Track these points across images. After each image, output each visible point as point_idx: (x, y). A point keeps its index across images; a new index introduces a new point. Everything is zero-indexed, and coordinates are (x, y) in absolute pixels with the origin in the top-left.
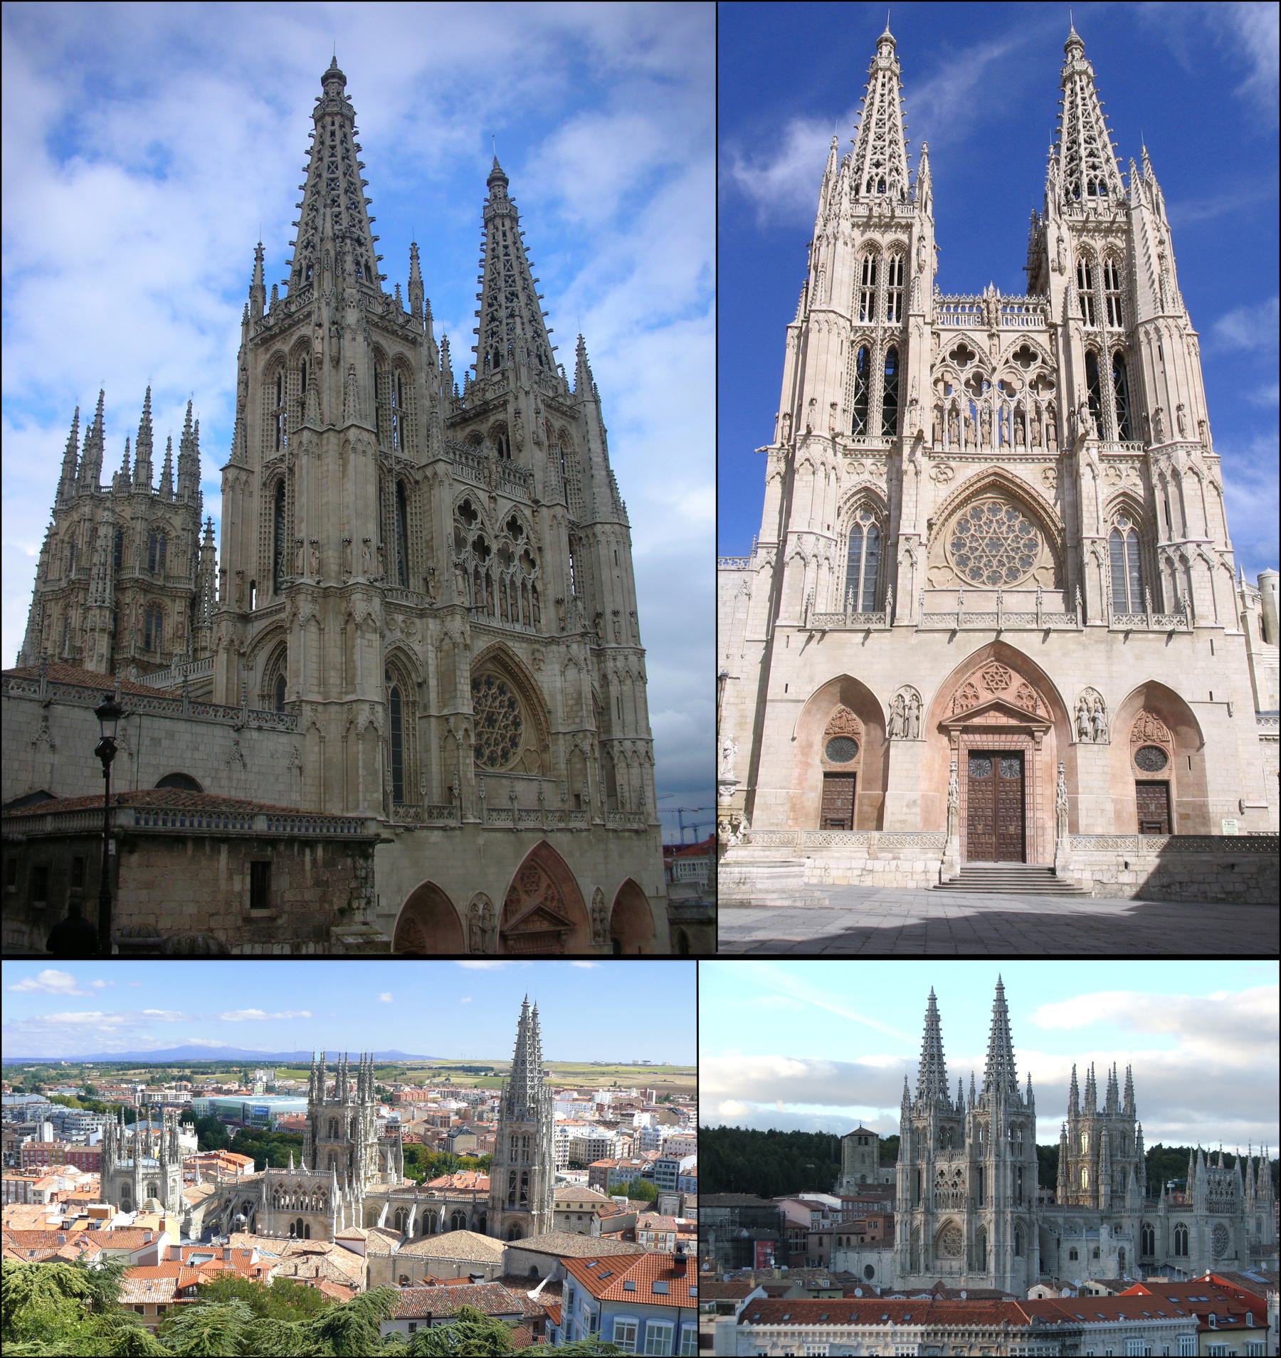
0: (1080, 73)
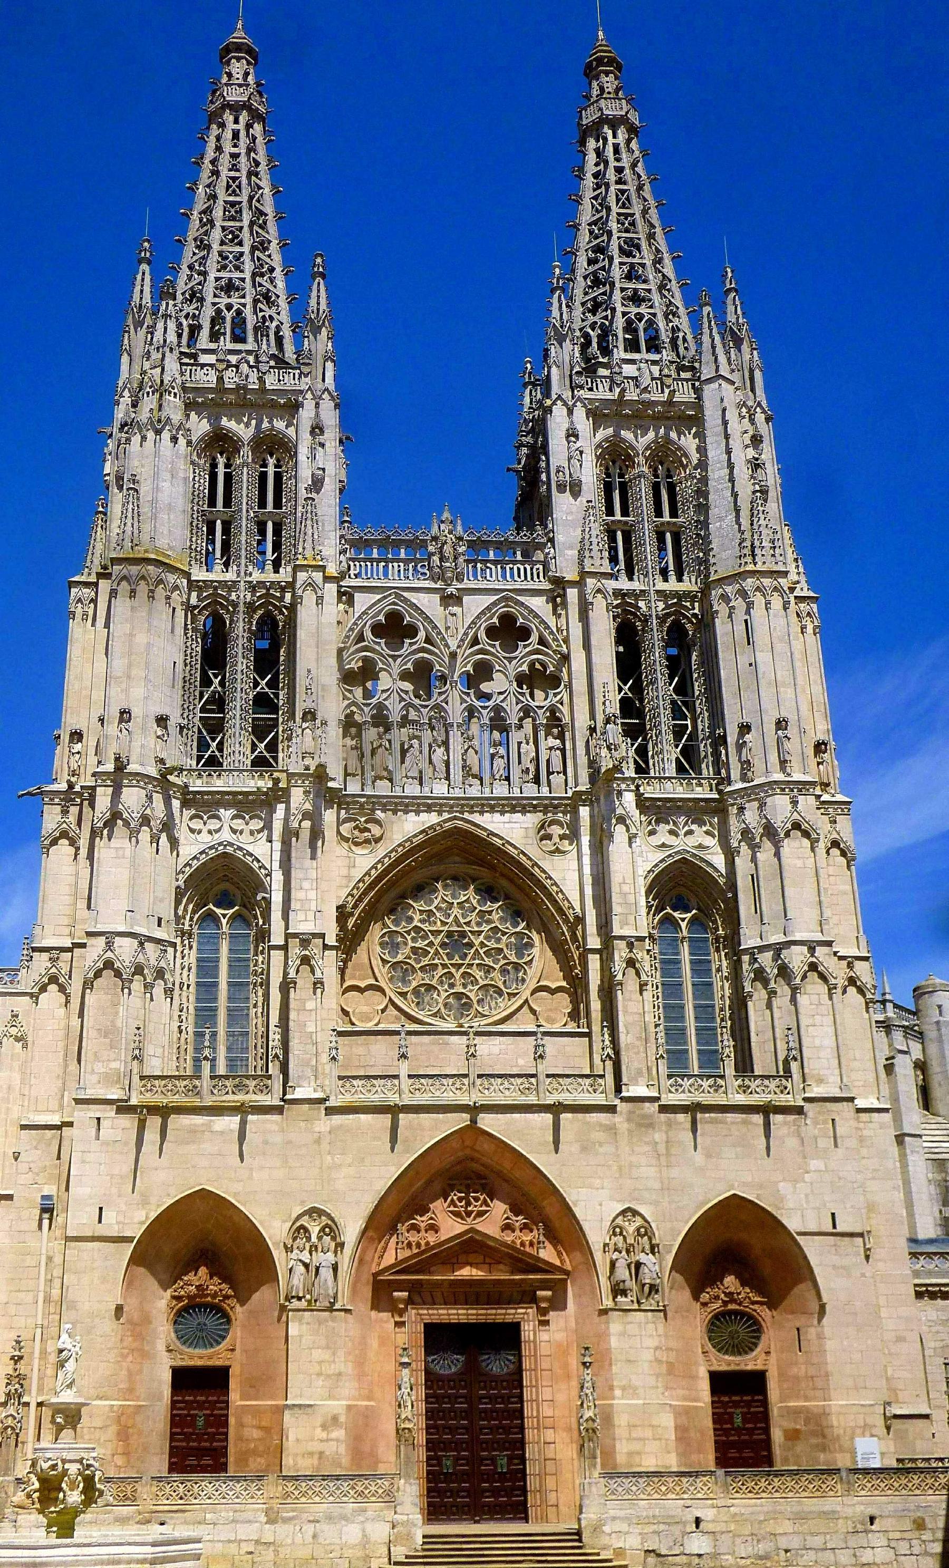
0: (614, 124)
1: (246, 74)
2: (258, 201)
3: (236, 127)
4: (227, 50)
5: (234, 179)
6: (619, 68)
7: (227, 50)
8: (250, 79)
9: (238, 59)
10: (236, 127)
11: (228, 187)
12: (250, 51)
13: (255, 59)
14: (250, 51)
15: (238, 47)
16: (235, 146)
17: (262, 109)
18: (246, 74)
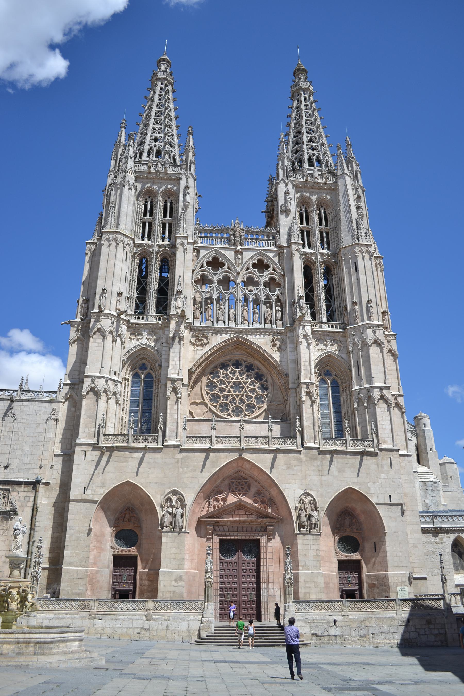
1: (166, 69)
2: (169, 111)
3: (162, 86)
4: (160, 61)
5: (160, 103)
6: (306, 72)
7: (160, 61)
8: (168, 70)
9: (164, 64)
10: (162, 86)
11: (157, 105)
12: (168, 62)
13: (170, 65)
14: (168, 62)
15: (164, 60)
16: (161, 92)
17: (172, 81)
18: (166, 69)
